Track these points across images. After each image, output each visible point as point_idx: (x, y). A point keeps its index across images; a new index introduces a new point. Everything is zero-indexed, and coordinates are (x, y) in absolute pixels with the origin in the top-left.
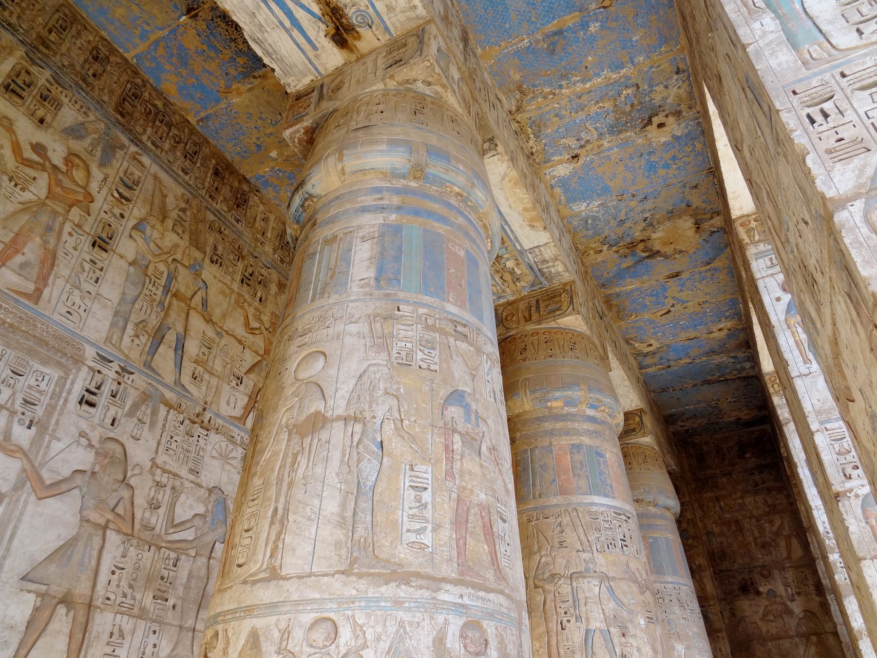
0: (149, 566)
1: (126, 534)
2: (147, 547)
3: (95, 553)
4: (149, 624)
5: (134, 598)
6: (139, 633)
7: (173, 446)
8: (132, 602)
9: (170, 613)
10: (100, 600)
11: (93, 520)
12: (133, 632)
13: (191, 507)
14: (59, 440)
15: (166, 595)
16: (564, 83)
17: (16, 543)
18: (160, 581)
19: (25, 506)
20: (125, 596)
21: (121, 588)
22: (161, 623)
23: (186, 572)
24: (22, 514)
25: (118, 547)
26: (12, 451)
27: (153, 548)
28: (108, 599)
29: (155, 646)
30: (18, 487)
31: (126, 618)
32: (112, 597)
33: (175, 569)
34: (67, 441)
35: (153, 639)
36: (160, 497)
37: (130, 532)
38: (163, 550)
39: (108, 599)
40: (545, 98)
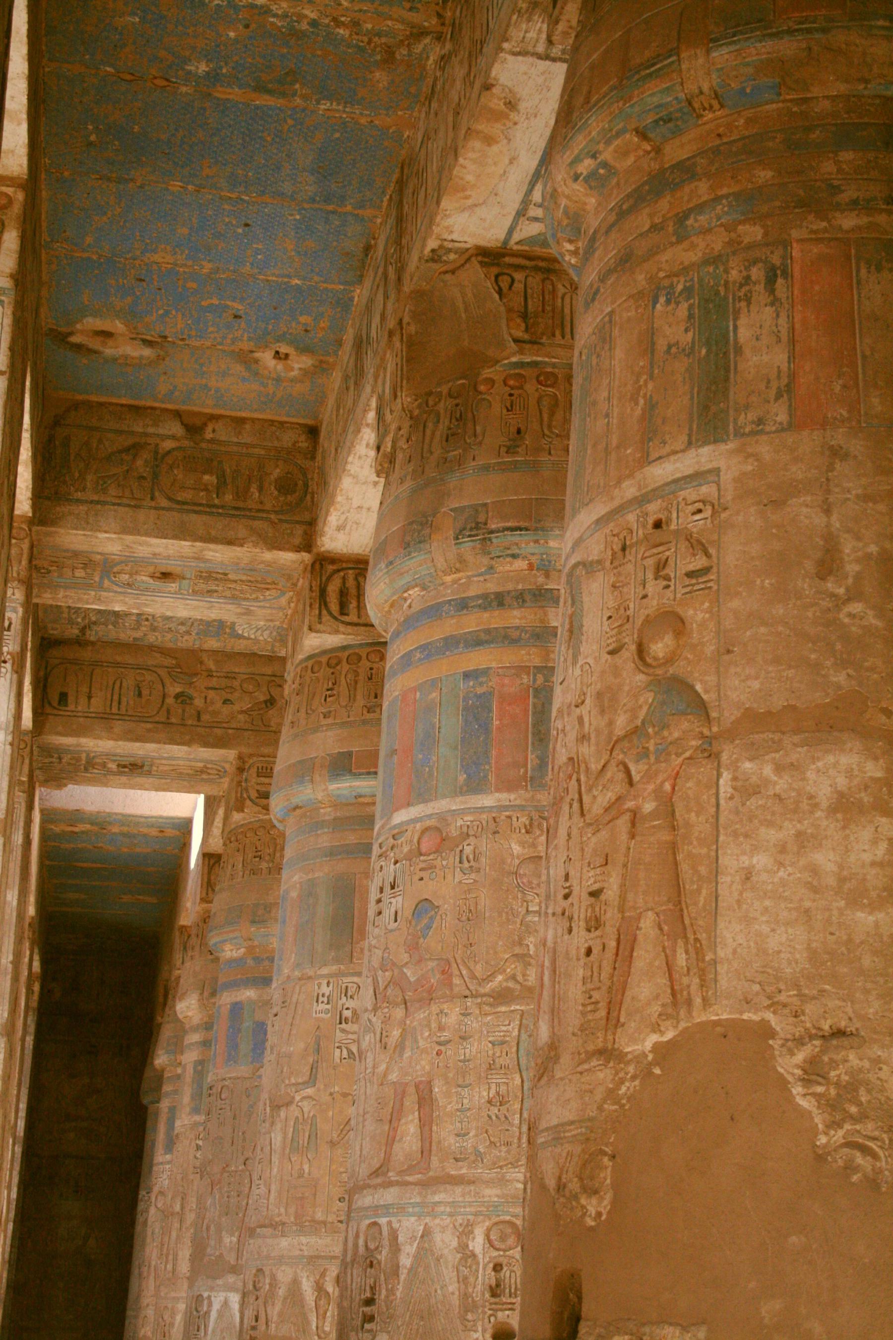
16: (304, 26)
40: (356, 24)
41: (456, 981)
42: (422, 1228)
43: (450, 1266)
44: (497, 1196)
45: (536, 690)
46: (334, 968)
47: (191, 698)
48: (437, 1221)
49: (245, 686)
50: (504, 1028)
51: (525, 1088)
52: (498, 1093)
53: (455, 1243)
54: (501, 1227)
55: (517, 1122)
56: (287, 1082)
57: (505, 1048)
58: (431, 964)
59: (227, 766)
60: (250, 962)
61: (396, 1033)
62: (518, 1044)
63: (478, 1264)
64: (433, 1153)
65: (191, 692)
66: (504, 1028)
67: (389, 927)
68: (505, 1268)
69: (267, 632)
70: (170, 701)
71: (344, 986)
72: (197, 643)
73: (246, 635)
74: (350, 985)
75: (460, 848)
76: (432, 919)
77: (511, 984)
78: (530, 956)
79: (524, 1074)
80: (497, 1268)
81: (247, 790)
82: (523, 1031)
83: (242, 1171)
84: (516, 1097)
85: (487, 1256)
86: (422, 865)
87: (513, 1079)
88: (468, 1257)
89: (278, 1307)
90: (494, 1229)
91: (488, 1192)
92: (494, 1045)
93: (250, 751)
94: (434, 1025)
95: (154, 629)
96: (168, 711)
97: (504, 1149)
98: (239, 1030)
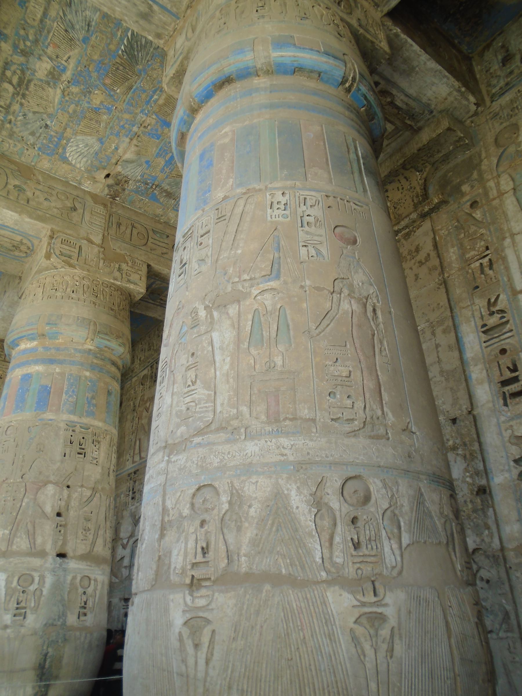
46: (289, 183)
47: (25, 190)
49: (59, 196)
56: (237, 280)
59: (36, 242)
60: (41, 349)
65: (24, 187)
69: (85, 159)
70: (10, 187)
71: (302, 198)
72: (35, 160)
73: (70, 159)
74: (308, 197)
81: (54, 250)
83: (20, 482)
89: (250, 532)
93: (59, 229)
95: (11, 135)
96: (8, 192)
98: (28, 390)
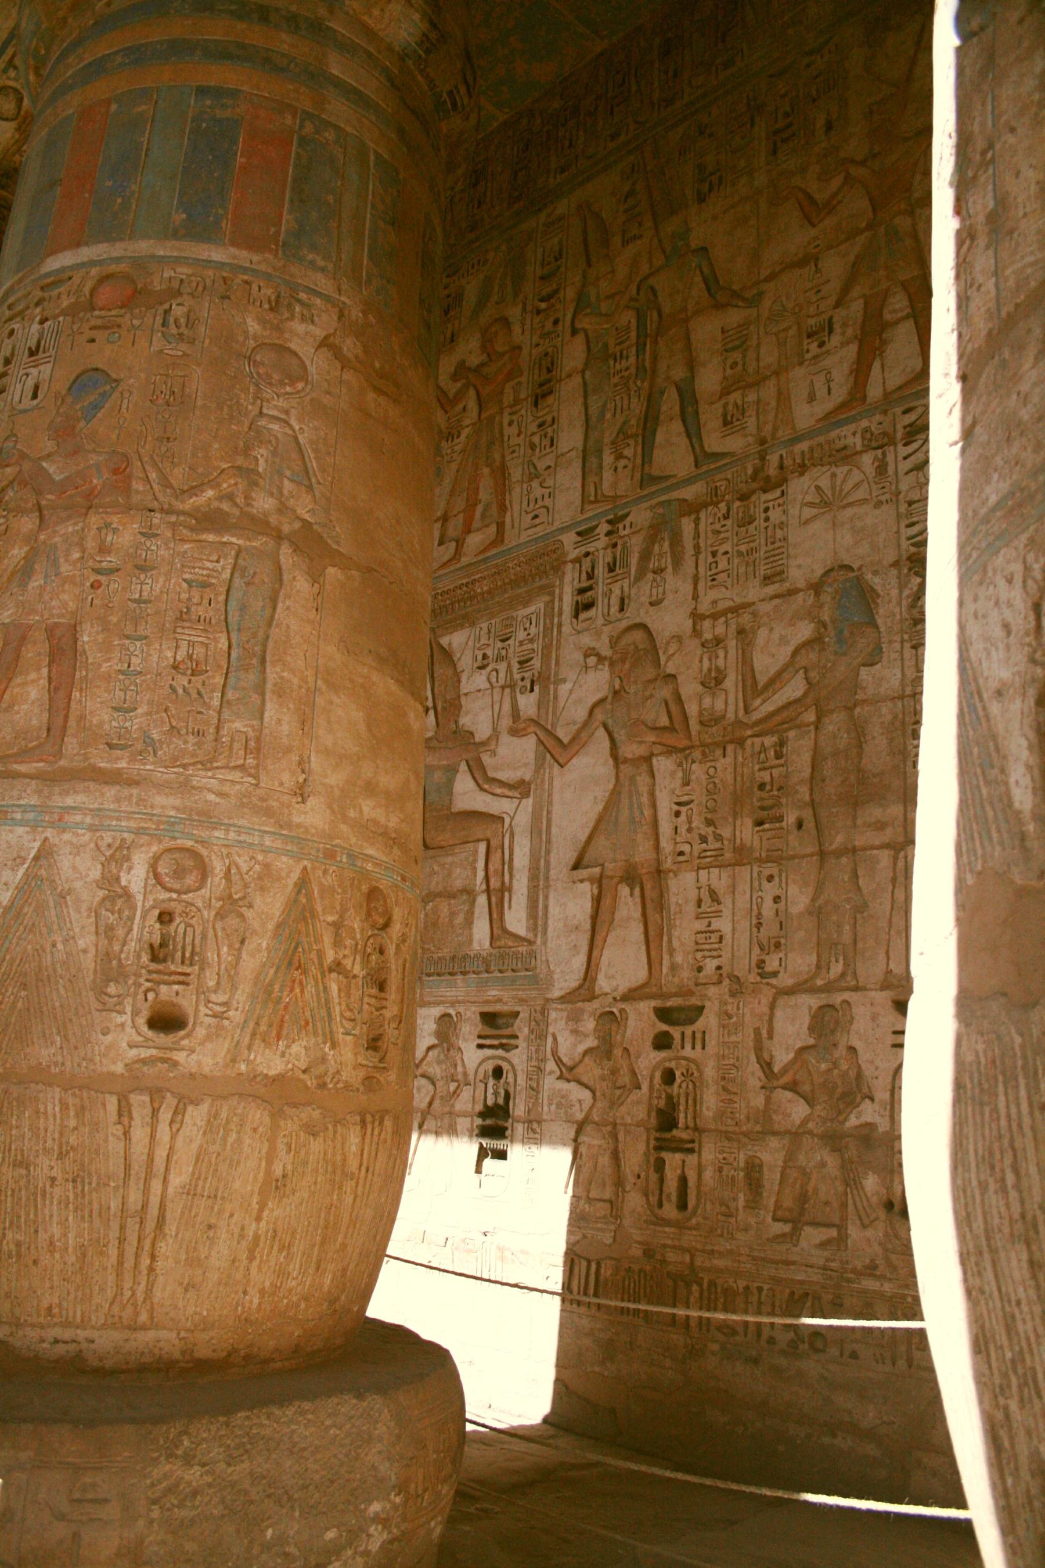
0: (730, 778)
1: (683, 750)
2: (719, 752)
3: (645, 799)
4: (756, 869)
5: (718, 838)
6: (744, 887)
7: (723, 564)
8: (718, 845)
9: (794, 840)
10: (669, 860)
11: (630, 756)
12: (733, 889)
13: (783, 640)
14: (564, 681)
15: (776, 812)
17: (554, 830)
18: (758, 793)
19: (551, 784)
20: (704, 839)
21: (696, 831)
22: (778, 861)
23: (806, 757)
24: (550, 795)
25: (673, 774)
26: (524, 729)
27: (730, 748)
28: (681, 853)
29: (777, 899)
30: (539, 766)
31: (715, 871)
32: (686, 848)
33: (782, 761)
34: (572, 676)
35: (770, 890)
36: (721, 662)
37: (686, 743)
38: (749, 742)
39: (681, 853)
41: (137, 486)
42: (37, 845)
43: (84, 907)
44: (177, 809)
45: (303, 141)
48: (67, 836)
50: (209, 565)
51: (234, 655)
52: (190, 657)
53: (96, 873)
54: (177, 855)
55: (216, 703)
57: (209, 593)
58: (93, 459)
61: (18, 552)
62: (228, 591)
63: (133, 908)
64: (69, 731)
66: (209, 565)
67: (21, 407)
68: (178, 920)
75: (166, 306)
76: (105, 396)
77: (225, 506)
78: (258, 474)
79: (234, 636)
80: (165, 917)
82: (237, 575)
84: (219, 666)
85: (151, 898)
86: (93, 322)
87: (216, 640)
88: (116, 895)
90: (166, 858)
91: (159, 800)
92: (190, 586)
94: (91, 544)
97: (192, 739)
